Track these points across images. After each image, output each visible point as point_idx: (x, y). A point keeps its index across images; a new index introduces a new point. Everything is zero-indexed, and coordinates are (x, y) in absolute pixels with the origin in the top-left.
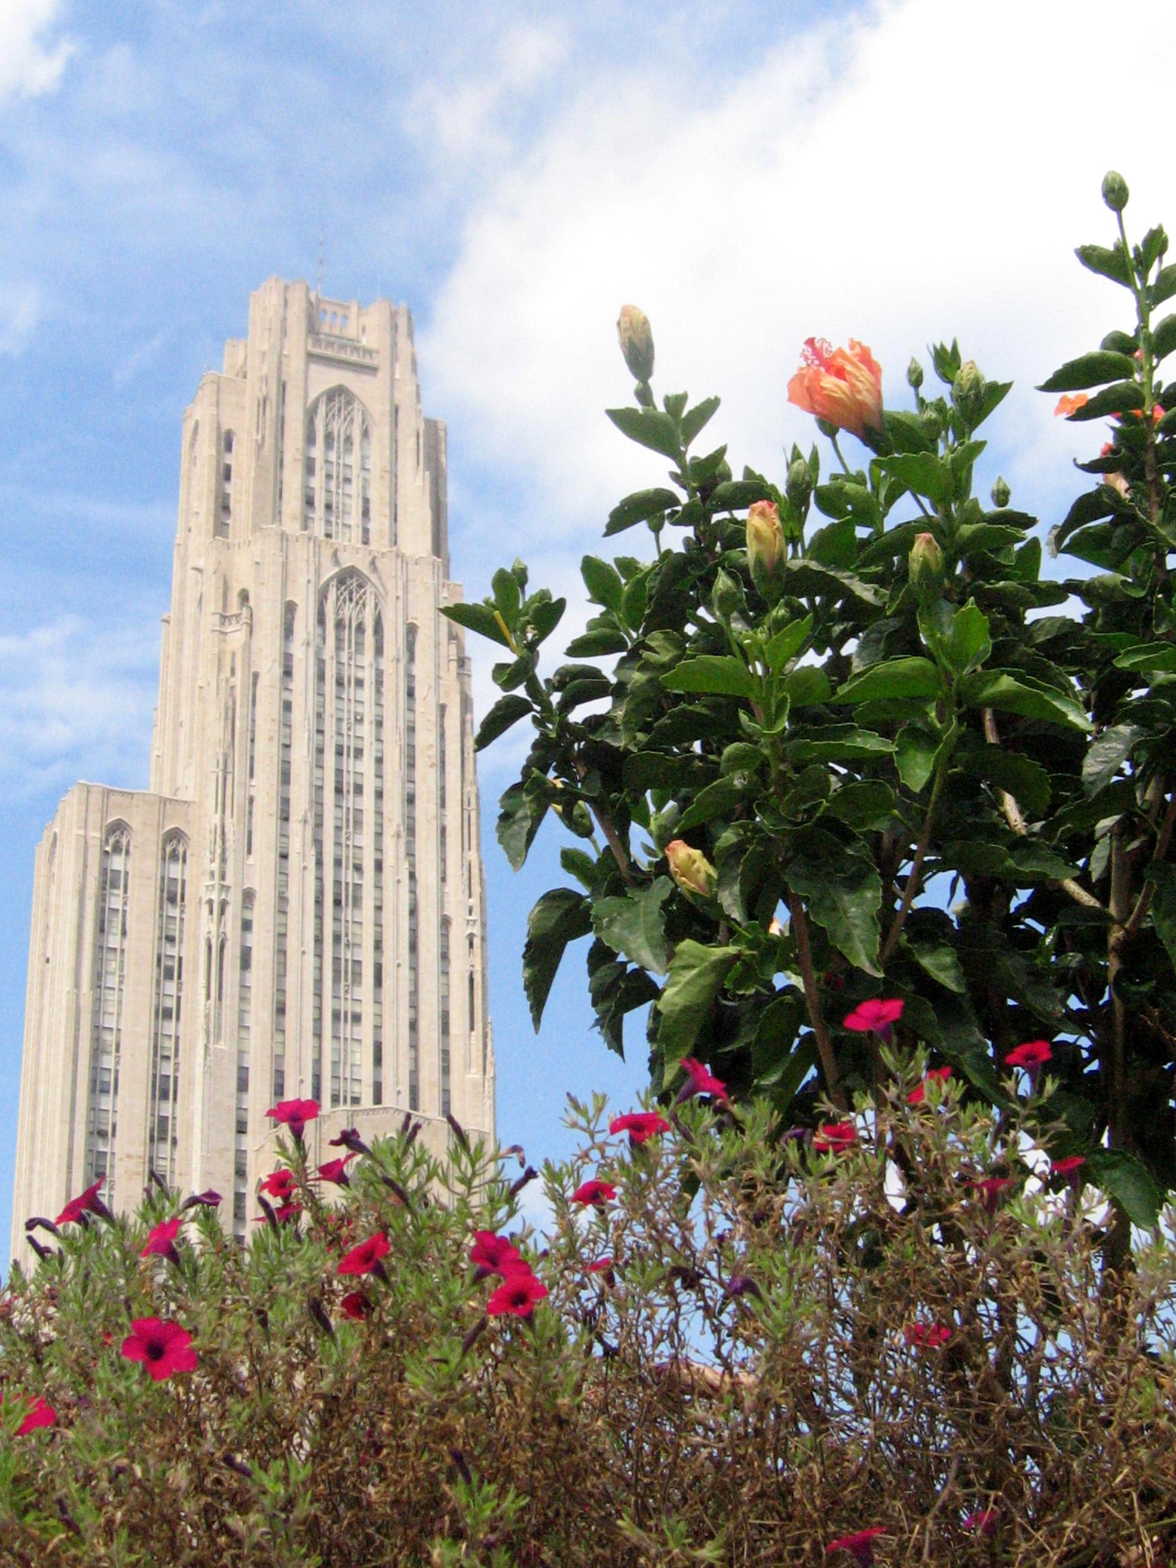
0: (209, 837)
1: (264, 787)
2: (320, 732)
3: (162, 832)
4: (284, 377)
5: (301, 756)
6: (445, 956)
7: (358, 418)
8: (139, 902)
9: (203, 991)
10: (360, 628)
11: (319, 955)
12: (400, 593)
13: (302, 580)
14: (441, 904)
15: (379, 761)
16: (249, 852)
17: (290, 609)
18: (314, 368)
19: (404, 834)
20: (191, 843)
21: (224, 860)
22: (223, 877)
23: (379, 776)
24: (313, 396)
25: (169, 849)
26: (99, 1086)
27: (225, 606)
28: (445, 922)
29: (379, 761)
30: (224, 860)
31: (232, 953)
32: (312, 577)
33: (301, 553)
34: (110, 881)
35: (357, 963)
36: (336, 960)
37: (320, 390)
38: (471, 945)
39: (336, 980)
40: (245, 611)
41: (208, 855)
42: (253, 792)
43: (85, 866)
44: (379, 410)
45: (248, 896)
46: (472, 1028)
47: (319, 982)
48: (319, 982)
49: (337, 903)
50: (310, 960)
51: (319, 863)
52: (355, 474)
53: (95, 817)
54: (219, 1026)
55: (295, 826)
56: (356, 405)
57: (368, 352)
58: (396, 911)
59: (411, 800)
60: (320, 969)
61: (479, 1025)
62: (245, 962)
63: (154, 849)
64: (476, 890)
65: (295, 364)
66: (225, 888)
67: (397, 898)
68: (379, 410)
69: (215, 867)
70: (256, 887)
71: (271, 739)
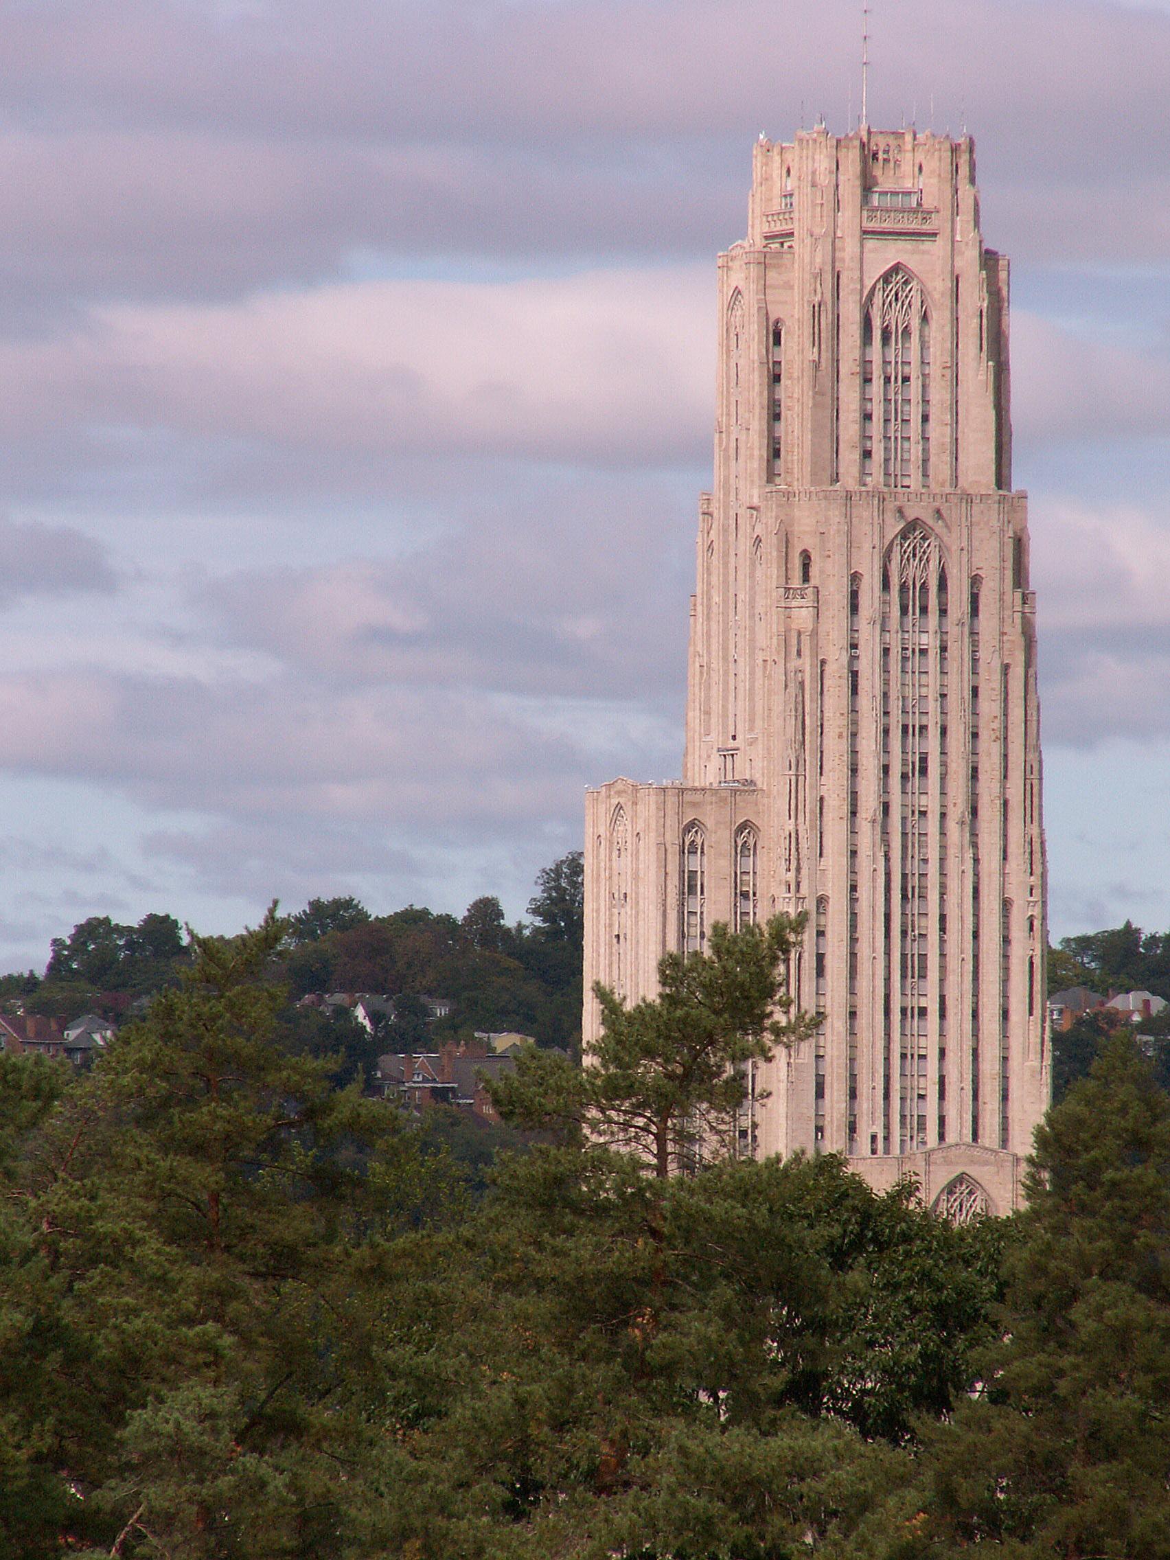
1: (834, 785)
2: (886, 713)
3: (734, 829)
6: (1006, 940)
11: (888, 953)
12: (965, 544)
13: (867, 546)
14: (1003, 889)
16: (821, 855)
18: (871, 244)
20: (761, 835)
21: (798, 870)
24: (869, 284)
28: (1006, 904)
30: (798, 870)
32: (876, 541)
35: (923, 957)
36: (904, 956)
38: (1031, 929)
39: (904, 977)
46: (1031, 1014)
47: (888, 980)
49: (904, 897)
52: (914, 371)
53: (671, 821)
56: (914, 283)
58: (961, 906)
59: (974, 773)
62: (820, 971)
63: (727, 846)
64: (1038, 869)
65: (850, 247)
67: (960, 891)
68: (939, 286)
69: (791, 876)
70: (829, 893)
71: (840, 736)
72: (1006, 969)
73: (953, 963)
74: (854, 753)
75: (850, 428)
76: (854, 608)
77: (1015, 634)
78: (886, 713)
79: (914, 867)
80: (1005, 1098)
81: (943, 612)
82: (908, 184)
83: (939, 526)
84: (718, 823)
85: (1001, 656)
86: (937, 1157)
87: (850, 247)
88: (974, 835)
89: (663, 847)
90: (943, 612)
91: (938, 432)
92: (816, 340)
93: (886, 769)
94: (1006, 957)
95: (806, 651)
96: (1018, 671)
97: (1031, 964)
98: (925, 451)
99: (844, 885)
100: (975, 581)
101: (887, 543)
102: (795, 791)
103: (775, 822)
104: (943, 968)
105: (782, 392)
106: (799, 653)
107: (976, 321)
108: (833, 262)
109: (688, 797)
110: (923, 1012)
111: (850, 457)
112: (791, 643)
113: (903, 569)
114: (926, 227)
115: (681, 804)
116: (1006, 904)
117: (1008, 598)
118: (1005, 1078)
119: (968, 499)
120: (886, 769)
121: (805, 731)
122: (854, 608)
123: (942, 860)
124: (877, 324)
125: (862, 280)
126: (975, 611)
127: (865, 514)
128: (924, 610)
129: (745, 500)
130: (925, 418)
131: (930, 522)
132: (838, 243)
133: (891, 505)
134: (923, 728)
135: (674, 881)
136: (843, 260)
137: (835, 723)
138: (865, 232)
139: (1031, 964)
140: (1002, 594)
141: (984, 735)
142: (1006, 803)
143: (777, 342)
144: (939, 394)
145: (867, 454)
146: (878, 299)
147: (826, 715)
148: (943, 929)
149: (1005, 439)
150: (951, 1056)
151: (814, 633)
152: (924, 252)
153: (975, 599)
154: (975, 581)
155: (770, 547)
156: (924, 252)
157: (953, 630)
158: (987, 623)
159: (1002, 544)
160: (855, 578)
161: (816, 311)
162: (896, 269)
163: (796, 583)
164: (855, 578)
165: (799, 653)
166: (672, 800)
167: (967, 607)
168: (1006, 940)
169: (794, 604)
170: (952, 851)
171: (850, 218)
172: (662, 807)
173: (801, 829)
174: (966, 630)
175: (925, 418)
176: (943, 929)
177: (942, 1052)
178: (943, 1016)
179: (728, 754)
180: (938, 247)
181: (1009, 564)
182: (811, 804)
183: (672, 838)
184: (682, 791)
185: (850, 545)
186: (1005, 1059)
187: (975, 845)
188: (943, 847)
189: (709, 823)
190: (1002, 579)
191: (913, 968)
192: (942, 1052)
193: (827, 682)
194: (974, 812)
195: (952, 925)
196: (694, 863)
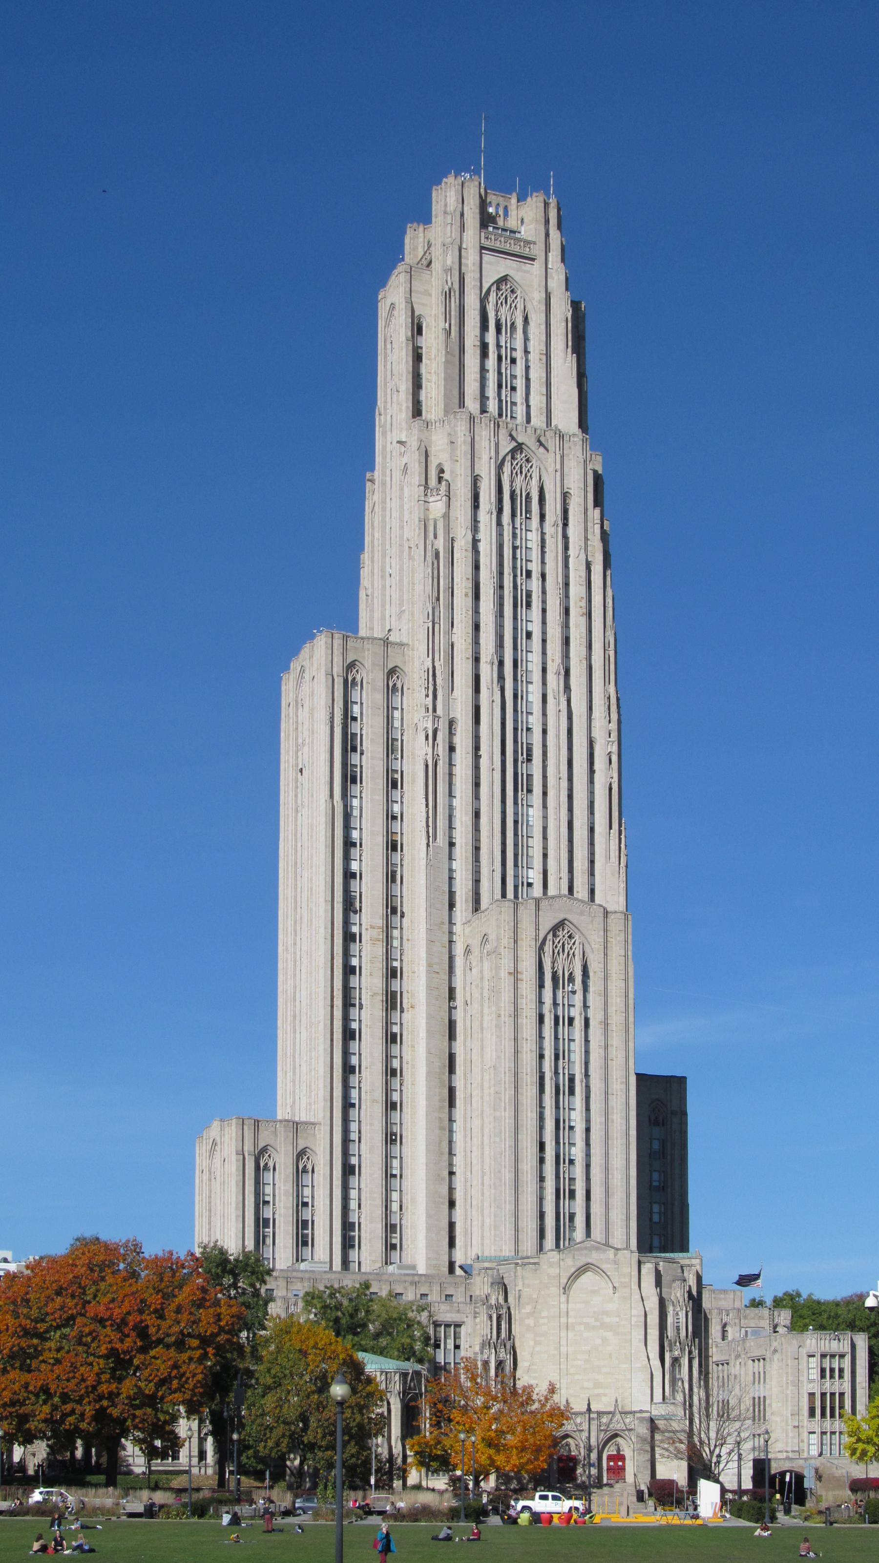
3: (386, 671)
17: (475, 480)
18: (487, 258)
22: (435, 710)
24: (486, 287)
33: (484, 435)
52: (519, 355)
57: (527, 243)
65: (471, 258)
66: (436, 718)
81: (542, 517)
84: (374, 665)
86: (544, 904)
87: (471, 258)
90: (542, 517)
101: (500, 458)
102: (432, 633)
103: (416, 666)
105: (423, 341)
107: (564, 324)
121: (440, 595)
133: (503, 432)
136: (467, 265)
138: (482, 248)
146: (492, 298)
152: (526, 272)
156: (526, 272)
169: (431, 499)
173: (437, 664)
180: (537, 268)
183: (338, 669)
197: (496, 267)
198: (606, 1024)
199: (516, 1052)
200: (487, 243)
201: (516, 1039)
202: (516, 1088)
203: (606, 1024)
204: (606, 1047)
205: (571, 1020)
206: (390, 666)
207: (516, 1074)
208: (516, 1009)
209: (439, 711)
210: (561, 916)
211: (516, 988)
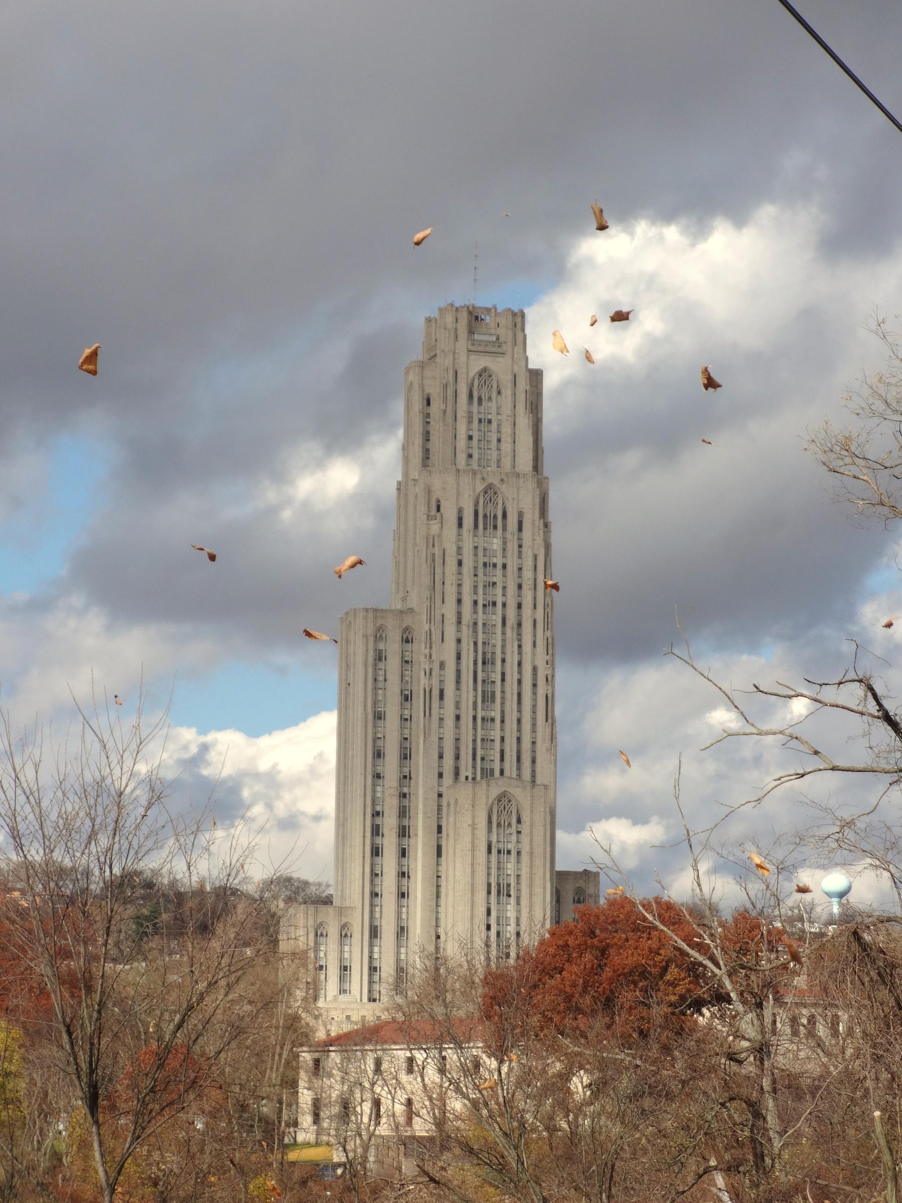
0: (424, 635)
1: (450, 610)
2: (476, 575)
4: (457, 367)
5: (467, 589)
6: (535, 685)
7: (495, 386)
8: (393, 664)
9: (422, 714)
10: (495, 517)
11: (475, 689)
12: (515, 496)
13: (466, 496)
14: (533, 660)
15: (504, 588)
16: (443, 641)
18: (472, 357)
19: (515, 626)
21: (431, 648)
23: (504, 595)
24: (471, 375)
25: (405, 637)
26: (378, 754)
27: (429, 511)
28: (535, 669)
29: (504, 588)
30: (431, 648)
31: (436, 693)
32: (471, 493)
34: (380, 657)
35: (493, 693)
36: (483, 692)
37: (475, 372)
39: (483, 701)
40: (439, 515)
41: (423, 645)
42: (444, 611)
43: (367, 650)
44: (506, 379)
45: (442, 665)
47: (475, 703)
48: (475, 703)
49: (484, 663)
50: (472, 693)
51: (475, 644)
54: (430, 730)
55: (464, 629)
58: (512, 668)
59: (519, 606)
60: (476, 696)
61: (550, 720)
63: (399, 639)
64: (550, 652)
68: (506, 379)
69: (427, 651)
72: (535, 700)
73: (508, 695)
74: (459, 593)
75: (462, 442)
76: (460, 525)
77: (540, 541)
78: (476, 575)
79: (489, 649)
80: (534, 761)
82: (493, 331)
83: (503, 488)
85: (533, 550)
87: (463, 358)
88: (519, 634)
89: (366, 637)
91: (506, 446)
92: (445, 399)
93: (475, 603)
94: (535, 693)
95: (436, 544)
96: (541, 558)
97: (547, 697)
98: (499, 455)
99: (453, 655)
100: (521, 515)
103: (421, 627)
104: (503, 698)
106: (433, 546)
108: (454, 364)
109: (378, 614)
110: (493, 720)
111: (462, 457)
112: (431, 541)
113: (485, 507)
114: (500, 350)
115: (375, 618)
116: (535, 669)
117: (537, 523)
118: (534, 751)
119: (518, 475)
120: (475, 603)
122: (460, 525)
123: (503, 646)
124: (475, 394)
125: (467, 373)
126: (520, 529)
127: (465, 480)
128: (495, 527)
129: (412, 477)
130: (499, 440)
131: (498, 485)
132: (457, 356)
134: (494, 584)
135: (371, 653)
137: (451, 578)
139: (547, 697)
140: (534, 521)
141: (524, 587)
142: (535, 621)
143: (428, 404)
144: (507, 429)
145: (470, 456)
147: (446, 574)
148: (503, 680)
149: (540, 453)
150: (507, 740)
151: (440, 536)
153: (520, 524)
154: (521, 515)
155: (422, 500)
157: (509, 537)
158: (527, 534)
159: (534, 497)
160: (460, 511)
161: (445, 386)
162: (485, 370)
163: (434, 511)
164: (460, 511)
165: (433, 546)
166: (370, 615)
167: (516, 526)
168: (535, 685)
169: (432, 522)
170: (508, 641)
171: (462, 345)
172: (366, 618)
174: (516, 537)
175: (499, 440)
176: (503, 680)
177: (503, 739)
178: (503, 721)
179: (404, 599)
181: (537, 507)
182: (439, 618)
183: (371, 631)
184: (376, 610)
185: (458, 493)
186: (534, 743)
187: (520, 640)
188: (504, 640)
189: (390, 626)
190: (533, 513)
191: (488, 698)
192: (503, 739)
193: (446, 559)
194: (519, 625)
195: (508, 677)
196: (381, 646)
197: (478, 363)
198: (531, 853)
199: (473, 872)
200: (473, 348)
201: (473, 864)
202: (472, 893)
203: (531, 853)
204: (531, 867)
205: (509, 852)
206: (405, 626)
207: (473, 885)
208: (473, 846)
209: (434, 657)
210: (503, 789)
211: (473, 834)
